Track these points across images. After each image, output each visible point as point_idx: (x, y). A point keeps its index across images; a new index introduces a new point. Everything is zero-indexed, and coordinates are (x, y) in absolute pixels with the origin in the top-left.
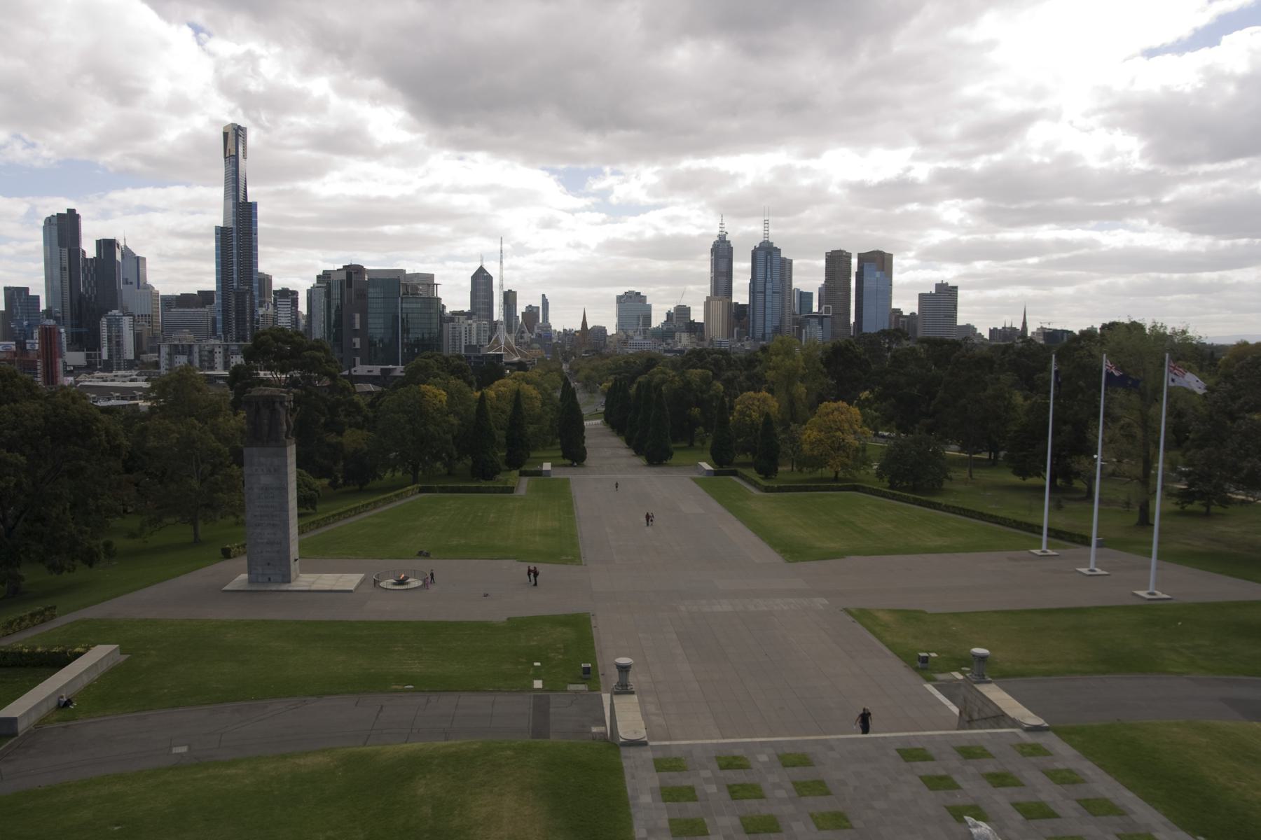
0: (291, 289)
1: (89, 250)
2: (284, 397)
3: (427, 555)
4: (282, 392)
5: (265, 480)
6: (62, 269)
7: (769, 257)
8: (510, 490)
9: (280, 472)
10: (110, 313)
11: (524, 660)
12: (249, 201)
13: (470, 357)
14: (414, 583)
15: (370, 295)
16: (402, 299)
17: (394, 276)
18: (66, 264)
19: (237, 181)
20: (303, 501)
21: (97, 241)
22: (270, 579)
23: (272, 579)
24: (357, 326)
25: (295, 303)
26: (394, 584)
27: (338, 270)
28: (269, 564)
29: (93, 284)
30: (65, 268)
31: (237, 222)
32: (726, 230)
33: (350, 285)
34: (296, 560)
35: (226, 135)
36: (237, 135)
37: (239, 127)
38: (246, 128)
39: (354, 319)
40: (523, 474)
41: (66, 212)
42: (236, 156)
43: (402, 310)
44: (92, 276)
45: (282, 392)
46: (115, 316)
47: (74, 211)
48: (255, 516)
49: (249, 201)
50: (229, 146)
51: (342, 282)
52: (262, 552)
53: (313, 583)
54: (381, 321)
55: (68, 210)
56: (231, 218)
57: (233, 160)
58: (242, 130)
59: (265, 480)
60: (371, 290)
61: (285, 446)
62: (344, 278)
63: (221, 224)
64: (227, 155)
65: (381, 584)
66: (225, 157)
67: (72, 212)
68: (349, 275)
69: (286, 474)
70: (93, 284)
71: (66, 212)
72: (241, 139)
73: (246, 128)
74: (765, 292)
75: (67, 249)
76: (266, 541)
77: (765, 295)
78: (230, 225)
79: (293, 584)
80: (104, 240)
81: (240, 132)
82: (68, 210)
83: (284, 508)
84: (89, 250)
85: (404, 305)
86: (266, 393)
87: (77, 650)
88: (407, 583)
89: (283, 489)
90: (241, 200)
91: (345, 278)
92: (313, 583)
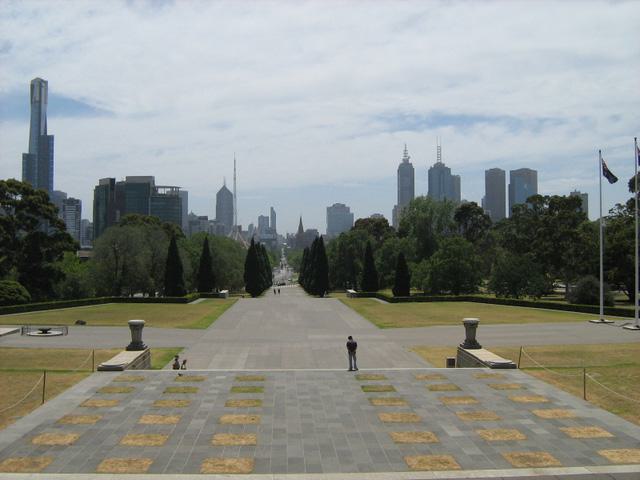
11: (35, 333)
12: (49, 134)
17: (146, 181)
33: (112, 189)
35: (32, 87)
37: (42, 81)
42: (40, 101)
49: (49, 134)
51: (106, 186)
57: (37, 104)
62: (108, 183)
63: (27, 152)
72: (43, 89)
81: (43, 84)
85: (155, 203)
90: (42, 134)
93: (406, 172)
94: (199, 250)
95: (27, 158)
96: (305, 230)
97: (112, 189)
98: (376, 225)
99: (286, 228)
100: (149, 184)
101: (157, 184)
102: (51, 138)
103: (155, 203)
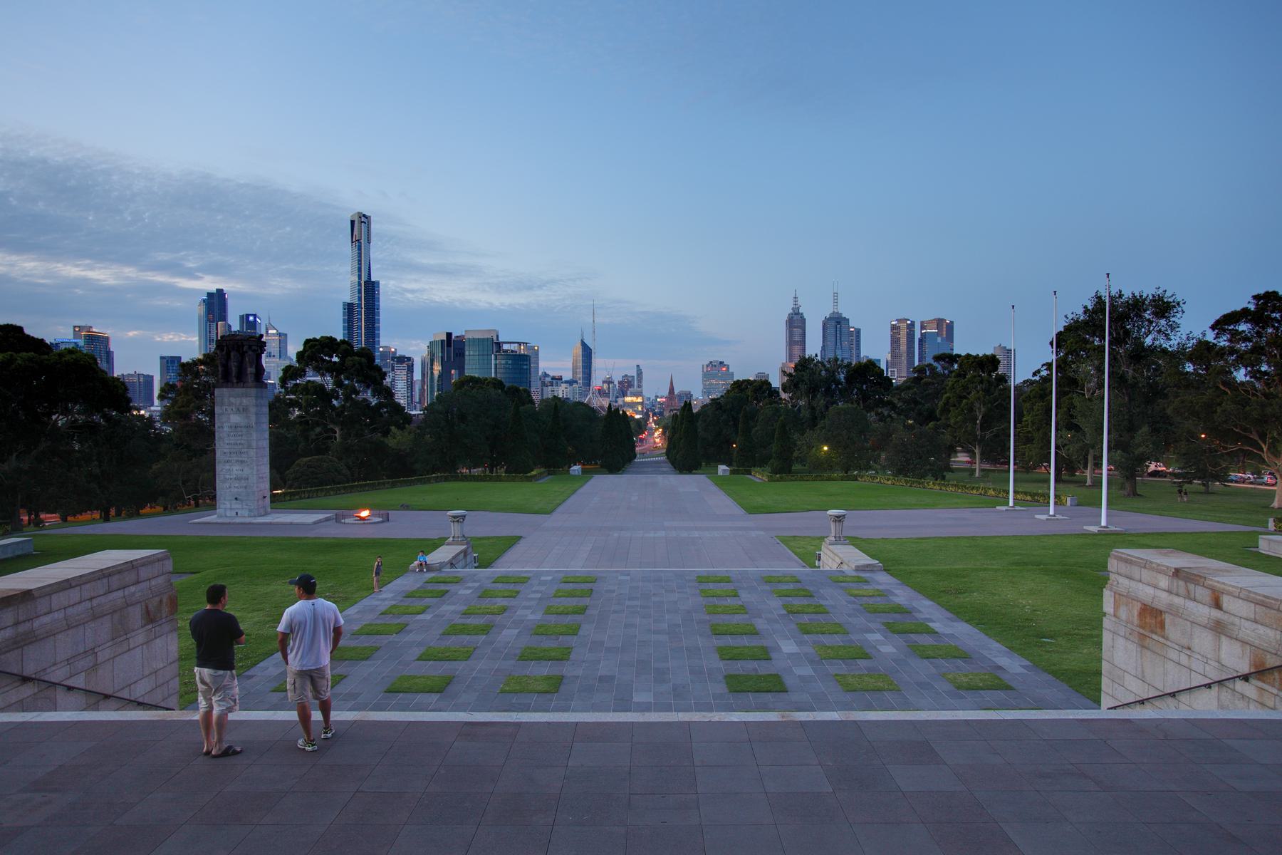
0: (407, 356)
12: (373, 280)
16: (496, 356)
22: (237, 513)
25: (410, 369)
28: (236, 499)
30: (213, 340)
34: (265, 497)
35: (353, 223)
38: (370, 217)
43: (496, 368)
48: (225, 453)
49: (373, 280)
50: (356, 232)
51: (442, 341)
52: (230, 487)
59: (235, 419)
64: (354, 240)
73: (370, 217)
91: (445, 339)
93: (796, 323)
95: (349, 309)
96: (676, 392)
98: (761, 387)
99: (655, 390)
101: (501, 340)
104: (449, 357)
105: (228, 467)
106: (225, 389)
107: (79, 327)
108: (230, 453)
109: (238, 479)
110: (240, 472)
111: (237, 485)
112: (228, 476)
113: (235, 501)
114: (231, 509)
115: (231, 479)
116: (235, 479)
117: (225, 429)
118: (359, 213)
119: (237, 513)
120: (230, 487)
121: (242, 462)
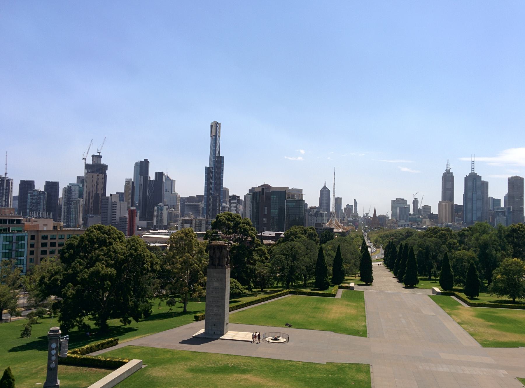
1: (152, 177)
2: (226, 245)
3: (290, 326)
4: (226, 243)
5: (216, 284)
6: (140, 185)
7: (474, 181)
8: (334, 296)
9: (223, 281)
10: (158, 204)
12: (220, 155)
13: (318, 229)
14: (282, 340)
15: (272, 199)
16: (287, 200)
18: (142, 183)
19: (215, 147)
20: (232, 296)
21: (155, 173)
22: (214, 332)
23: (215, 333)
24: (266, 213)
26: (272, 340)
27: (259, 187)
28: (214, 325)
29: (152, 192)
31: (215, 165)
32: (450, 167)
33: (263, 194)
35: (212, 126)
36: (216, 126)
38: (220, 123)
39: (264, 209)
40: (341, 288)
41: (143, 160)
42: (216, 136)
44: (152, 188)
45: (226, 243)
46: (160, 206)
47: (147, 160)
49: (220, 155)
51: (259, 192)
52: (212, 319)
53: (234, 336)
54: (277, 211)
55: (145, 159)
56: (213, 163)
58: (219, 124)
59: (216, 284)
60: (272, 196)
61: (226, 269)
62: (260, 190)
63: (208, 166)
64: (212, 135)
65: (267, 339)
66: (211, 136)
67: (146, 160)
68: (263, 189)
69: (225, 282)
70: (152, 192)
71: (143, 160)
73: (220, 123)
74: (472, 199)
75: (143, 176)
76: (214, 313)
77: (472, 201)
78: (212, 166)
79: (225, 335)
80: (158, 172)
81: (218, 125)
82: (145, 159)
83: (224, 299)
84: (152, 177)
85: (288, 204)
86: (219, 244)
87: (124, 361)
88: (279, 340)
89: (224, 289)
90: (217, 155)
92: (234, 336)
94: (334, 254)
95: (208, 170)
97: (263, 194)
100: (285, 192)
102: (222, 158)
103: (288, 204)
104: (262, 200)
105: (211, 309)
106: (212, 269)
107: (79, 177)
108: (213, 301)
109: (216, 315)
110: (217, 311)
111: (215, 318)
112: (211, 313)
113: (214, 326)
114: (211, 330)
115: (212, 315)
116: (214, 315)
117: (211, 289)
118: (215, 121)
119: (214, 332)
120: (212, 319)
121: (218, 306)
